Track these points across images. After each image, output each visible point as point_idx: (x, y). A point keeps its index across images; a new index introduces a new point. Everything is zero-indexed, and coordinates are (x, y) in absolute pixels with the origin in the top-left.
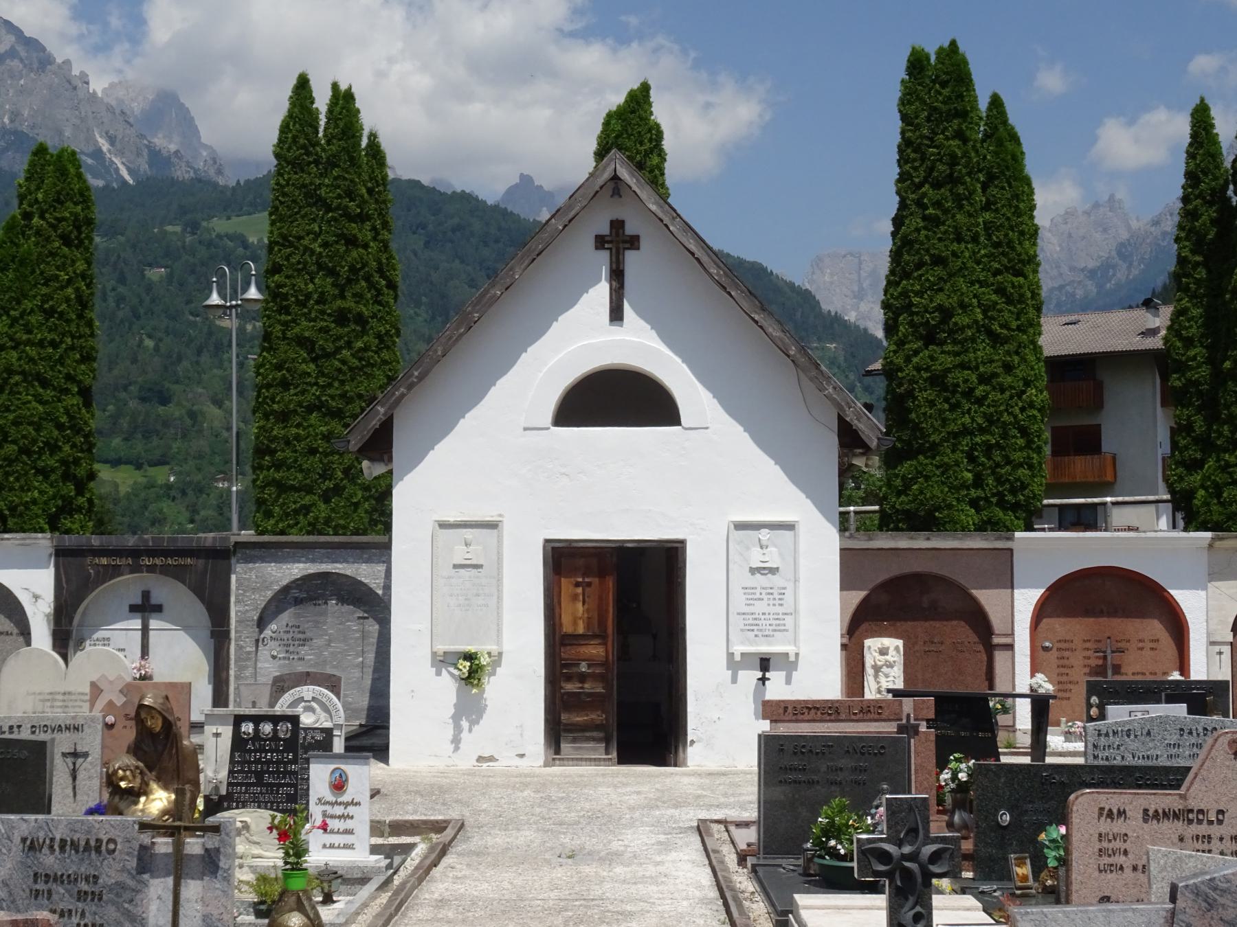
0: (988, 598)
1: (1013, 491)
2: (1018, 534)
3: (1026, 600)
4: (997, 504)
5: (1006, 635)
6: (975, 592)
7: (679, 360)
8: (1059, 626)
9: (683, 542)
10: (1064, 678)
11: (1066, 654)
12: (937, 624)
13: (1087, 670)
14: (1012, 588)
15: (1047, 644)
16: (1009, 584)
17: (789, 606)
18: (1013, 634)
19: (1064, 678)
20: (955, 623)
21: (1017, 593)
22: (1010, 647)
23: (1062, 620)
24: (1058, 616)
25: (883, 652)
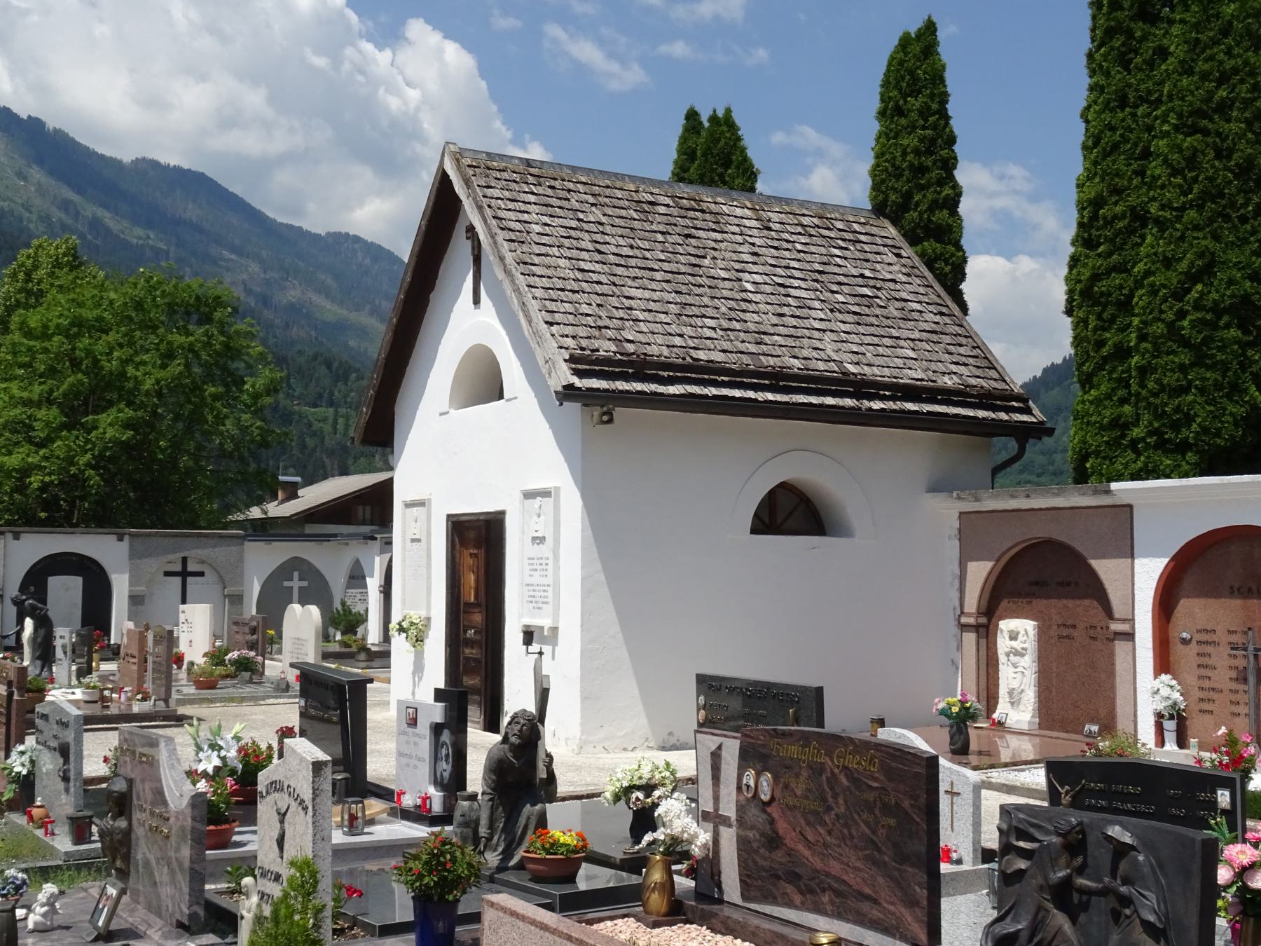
0: (1105, 568)
1: (1176, 427)
2: (1114, 486)
3: (1148, 572)
4: (1157, 447)
5: (1124, 620)
6: (1095, 563)
7: (503, 332)
8: (1194, 612)
9: (449, 516)
10: (1207, 684)
11: (1209, 649)
12: (1070, 603)
13: (1234, 674)
14: (1132, 557)
15: (1185, 635)
16: (1130, 553)
17: (549, 580)
18: (1133, 620)
19: (1207, 684)
20: (1087, 602)
21: (1138, 562)
22: (1130, 636)
23: (1203, 601)
24: (1198, 596)
25: (1013, 636)
